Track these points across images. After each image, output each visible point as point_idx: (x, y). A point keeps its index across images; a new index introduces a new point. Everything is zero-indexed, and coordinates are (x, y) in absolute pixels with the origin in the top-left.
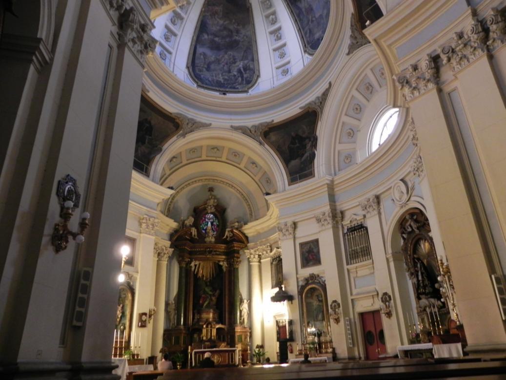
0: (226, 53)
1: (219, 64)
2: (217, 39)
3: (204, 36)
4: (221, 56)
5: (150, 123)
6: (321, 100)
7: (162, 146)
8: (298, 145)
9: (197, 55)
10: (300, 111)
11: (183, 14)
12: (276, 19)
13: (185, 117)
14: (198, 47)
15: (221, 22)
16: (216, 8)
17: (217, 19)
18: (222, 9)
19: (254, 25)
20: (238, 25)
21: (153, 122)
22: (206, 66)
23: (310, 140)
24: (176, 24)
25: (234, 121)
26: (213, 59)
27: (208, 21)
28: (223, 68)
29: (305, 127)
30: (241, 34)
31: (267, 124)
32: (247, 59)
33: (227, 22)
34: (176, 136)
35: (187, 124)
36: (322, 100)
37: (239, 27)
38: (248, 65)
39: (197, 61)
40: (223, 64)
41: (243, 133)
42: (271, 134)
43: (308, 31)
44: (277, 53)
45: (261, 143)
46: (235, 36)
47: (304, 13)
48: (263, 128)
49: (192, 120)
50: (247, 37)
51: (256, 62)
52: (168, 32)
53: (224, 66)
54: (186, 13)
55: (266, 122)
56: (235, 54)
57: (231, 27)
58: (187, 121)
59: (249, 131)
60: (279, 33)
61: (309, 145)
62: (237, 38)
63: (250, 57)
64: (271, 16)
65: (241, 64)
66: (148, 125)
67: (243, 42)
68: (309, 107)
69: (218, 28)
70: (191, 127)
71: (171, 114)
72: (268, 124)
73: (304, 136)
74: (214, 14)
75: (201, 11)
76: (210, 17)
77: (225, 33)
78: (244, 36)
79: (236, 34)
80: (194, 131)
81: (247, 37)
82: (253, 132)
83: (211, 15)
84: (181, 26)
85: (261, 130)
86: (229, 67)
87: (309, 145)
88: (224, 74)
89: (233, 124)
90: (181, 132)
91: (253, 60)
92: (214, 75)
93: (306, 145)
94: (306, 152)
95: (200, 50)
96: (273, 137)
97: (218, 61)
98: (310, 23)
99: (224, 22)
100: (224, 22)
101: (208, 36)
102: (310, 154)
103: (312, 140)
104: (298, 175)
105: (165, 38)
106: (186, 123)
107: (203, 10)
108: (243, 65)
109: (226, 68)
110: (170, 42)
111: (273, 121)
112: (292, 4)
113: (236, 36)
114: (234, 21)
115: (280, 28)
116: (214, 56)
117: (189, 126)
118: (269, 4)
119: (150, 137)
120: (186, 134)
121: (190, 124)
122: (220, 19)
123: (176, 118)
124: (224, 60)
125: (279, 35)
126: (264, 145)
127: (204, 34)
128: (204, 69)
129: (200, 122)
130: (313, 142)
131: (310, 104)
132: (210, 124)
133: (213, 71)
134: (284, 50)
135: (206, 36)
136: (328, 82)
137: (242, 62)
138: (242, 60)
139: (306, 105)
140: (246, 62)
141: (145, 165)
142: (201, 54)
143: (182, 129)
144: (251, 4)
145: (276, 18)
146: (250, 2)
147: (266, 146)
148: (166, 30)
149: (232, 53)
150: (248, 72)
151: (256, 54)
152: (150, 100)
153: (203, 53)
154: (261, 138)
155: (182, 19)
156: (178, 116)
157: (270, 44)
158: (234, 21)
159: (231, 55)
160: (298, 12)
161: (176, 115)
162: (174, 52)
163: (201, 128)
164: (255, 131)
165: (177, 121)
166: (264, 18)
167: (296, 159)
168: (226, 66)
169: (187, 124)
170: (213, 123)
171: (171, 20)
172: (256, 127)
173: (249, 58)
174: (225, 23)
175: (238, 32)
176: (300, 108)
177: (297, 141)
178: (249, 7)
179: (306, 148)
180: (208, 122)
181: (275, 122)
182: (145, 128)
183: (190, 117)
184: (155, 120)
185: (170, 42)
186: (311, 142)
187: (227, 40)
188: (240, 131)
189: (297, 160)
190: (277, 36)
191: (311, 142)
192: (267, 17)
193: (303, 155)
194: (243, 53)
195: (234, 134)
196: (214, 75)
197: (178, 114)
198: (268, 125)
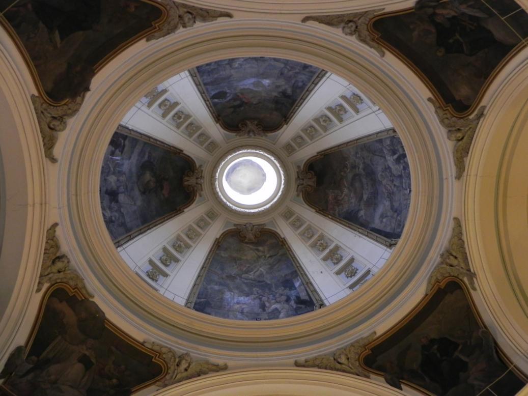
0: (380, 183)
1: (393, 193)
2: (365, 197)
3: (362, 216)
4: (384, 190)
5: (432, 341)
6: (343, 25)
7: (486, 327)
8: (458, 36)
9: (381, 228)
10: (388, 54)
11: (331, 247)
12: (323, 116)
13: (437, 268)
14: (373, 226)
15: (346, 191)
16: (330, 198)
17: (342, 197)
18: (331, 191)
19: (339, 146)
20: (346, 166)
21: (434, 335)
22: (395, 215)
23: (434, 14)
24: (341, 257)
25: (450, 174)
26: (387, 203)
27: (345, 210)
28: (397, 187)
29: (415, 33)
30: (355, 161)
31: (439, 111)
32: (382, 150)
33: (345, 183)
34: (472, 291)
35: (451, 266)
36: (342, 21)
37: (349, 166)
38: (387, 147)
39: (388, 230)
40: (393, 187)
41: (468, 153)
42: (457, 98)
43: (307, 70)
44: (359, 106)
45: (481, 115)
46: (360, 169)
47: (293, 81)
48: (449, 116)
49: (442, 255)
50: (357, 153)
51: (383, 136)
52: (346, 272)
53: (395, 185)
54: (331, 240)
55: (436, 112)
56: (380, 168)
57: (350, 176)
58: (445, 266)
59: (460, 143)
60: (336, 108)
61: (444, 12)
62: (361, 166)
63: (379, 146)
64: (322, 123)
65: (389, 158)
66: (436, 347)
67: (363, 158)
68: (373, 40)
69: (352, 195)
70: (456, 258)
71: (426, 295)
72: (438, 108)
73: (433, 30)
74: (338, 202)
75: (332, 219)
76: (341, 207)
77: (357, 185)
78: (356, 156)
79: (357, 168)
80: (466, 253)
81: (357, 153)
82: (460, 135)
83: (338, 206)
84: (344, 250)
85: (454, 119)
86: (394, 176)
87: (444, 12)
88: (404, 186)
89: (454, 174)
90: (466, 280)
91: (380, 141)
92: (405, 202)
93: (449, 19)
94: (463, 14)
95: (377, 223)
96: (463, 92)
97: (391, 195)
98: (297, 71)
99: (345, 187)
100: (345, 187)
101: (361, 210)
102: (461, 4)
103: (430, 11)
104: (503, 19)
105: (351, 277)
106: (448, 267)
107: (330, 217)
108: (391, 155)
109: (397, 183)
110: (357, 270)
111: (429, 100)
112: (296, 100)
113: (359, 168)
114: (342, 173)
115: (330, 109)
116: (385, 202)
117: (455, 262)
118: (310, 129)
119: (460, 348)
120: (469, 270)
121: (448, 261)
122: (342, 193)
123: (436, 288)
124: (388, 185)
125: (338, 108)
126: (482, 107)
127: (360, 215)
128: (399, 218)
129: (450, 242)
130: (434, 7)
131: (363, 41)
132: (457, 221)
133: (400, 204)
134: (350, 98)
135: (362, 213)
136: (303, 24)
137: (386, 157)
138: (385, 157)
139: (371, 47)
140: (385, 151)
141: (487, 387)
142: (382, 222)
143: (461, 278)
144: (318, 153)
145: (322, 116)
146: (316, 154)
147: (483, 103)
148: (343, 274)
149: (380, 173)
150: (396, 148)
151: (371, 137)
152: (389, 334)
153: (380, 218)
154: (471, 117)
155: (337, 248)
156: (433, 281)
157: (354, 119)
158: (342, 173)
159: (381, 175)
160: (298, 91)
161: (431, 286)
162: (369, 266)
163: (462, 238)
164: (459, 130)
165: (443, 285)
166: (327, 133)
167: (489, 32)
168: (394, 183)
169: (451, 266)
170: (454, 214)
171: (335, 264)
172: (452, 130)
173: (380, 147)
174: (346, 185)
175: (354, 167)
176: (383, 55)
177: (451, 41)
178: (321, 155)
179: (454, 17)
180: (452, 224)
181: (430, 95)
182: (438, 355)
183: (439, 259)
184: (431, 329)
185: (357, 270)
186: (438, 11)
187: (364, 180)
188: (465, 159)
189: (490, 27)
190: (340, 110)
191: (438, 11)
192: (325, 129)
193: (472, 18)
194: (376, 157)
195: (473, 172)
196: (405, 202)
197: (429, 282)
198: (440, 107)
